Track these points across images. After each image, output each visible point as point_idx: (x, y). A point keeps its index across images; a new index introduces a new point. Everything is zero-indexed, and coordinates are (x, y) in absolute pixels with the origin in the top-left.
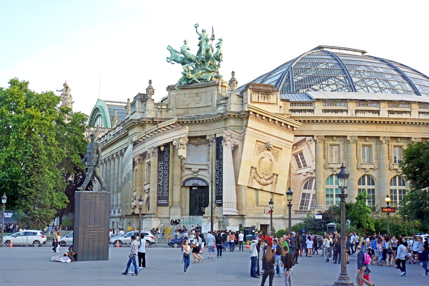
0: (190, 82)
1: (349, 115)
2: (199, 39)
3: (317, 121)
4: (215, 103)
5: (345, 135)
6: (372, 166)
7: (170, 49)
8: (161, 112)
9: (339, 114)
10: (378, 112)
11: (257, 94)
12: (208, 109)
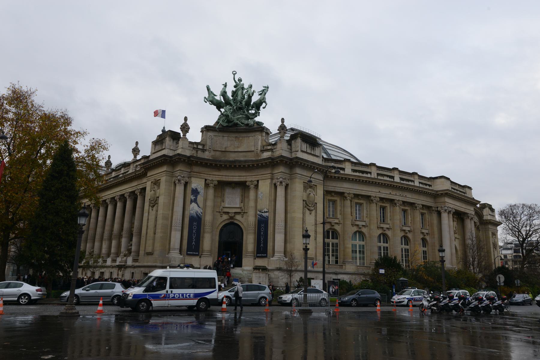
0: (230, 124)
1: (372, 176)
2: (235, 87)
3: (349, 179)
4: (259, 149)
5: (369, 194)
6: (388, 226)
8: (197, 151)
9: (365, 175)
10: (393, 177)
12: (249, 154)
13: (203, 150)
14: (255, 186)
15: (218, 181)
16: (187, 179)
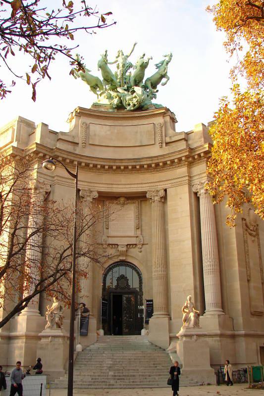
14: (161, 198)
15: (99, 192)
16: (49, 189)
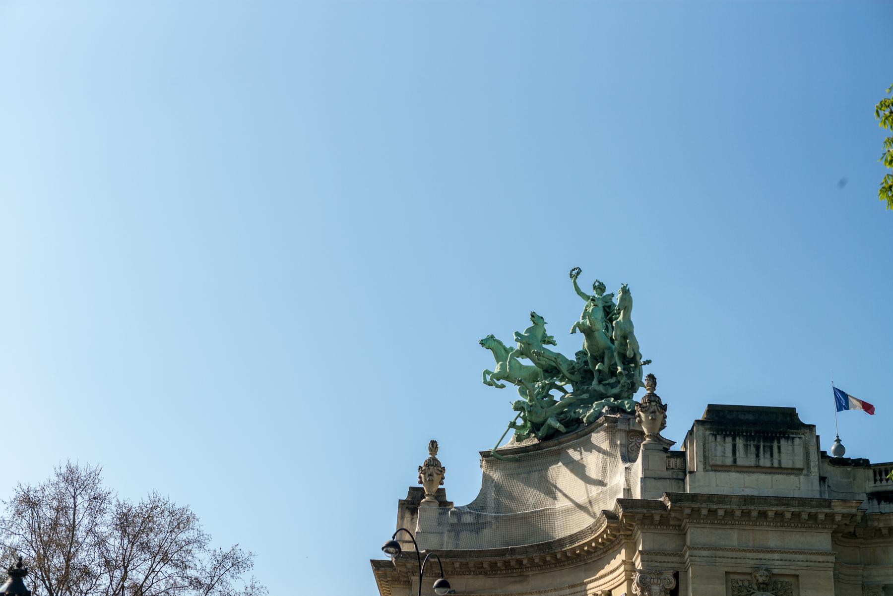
7: (489, 343)
11: (729, 440)
13: (478, 527)
